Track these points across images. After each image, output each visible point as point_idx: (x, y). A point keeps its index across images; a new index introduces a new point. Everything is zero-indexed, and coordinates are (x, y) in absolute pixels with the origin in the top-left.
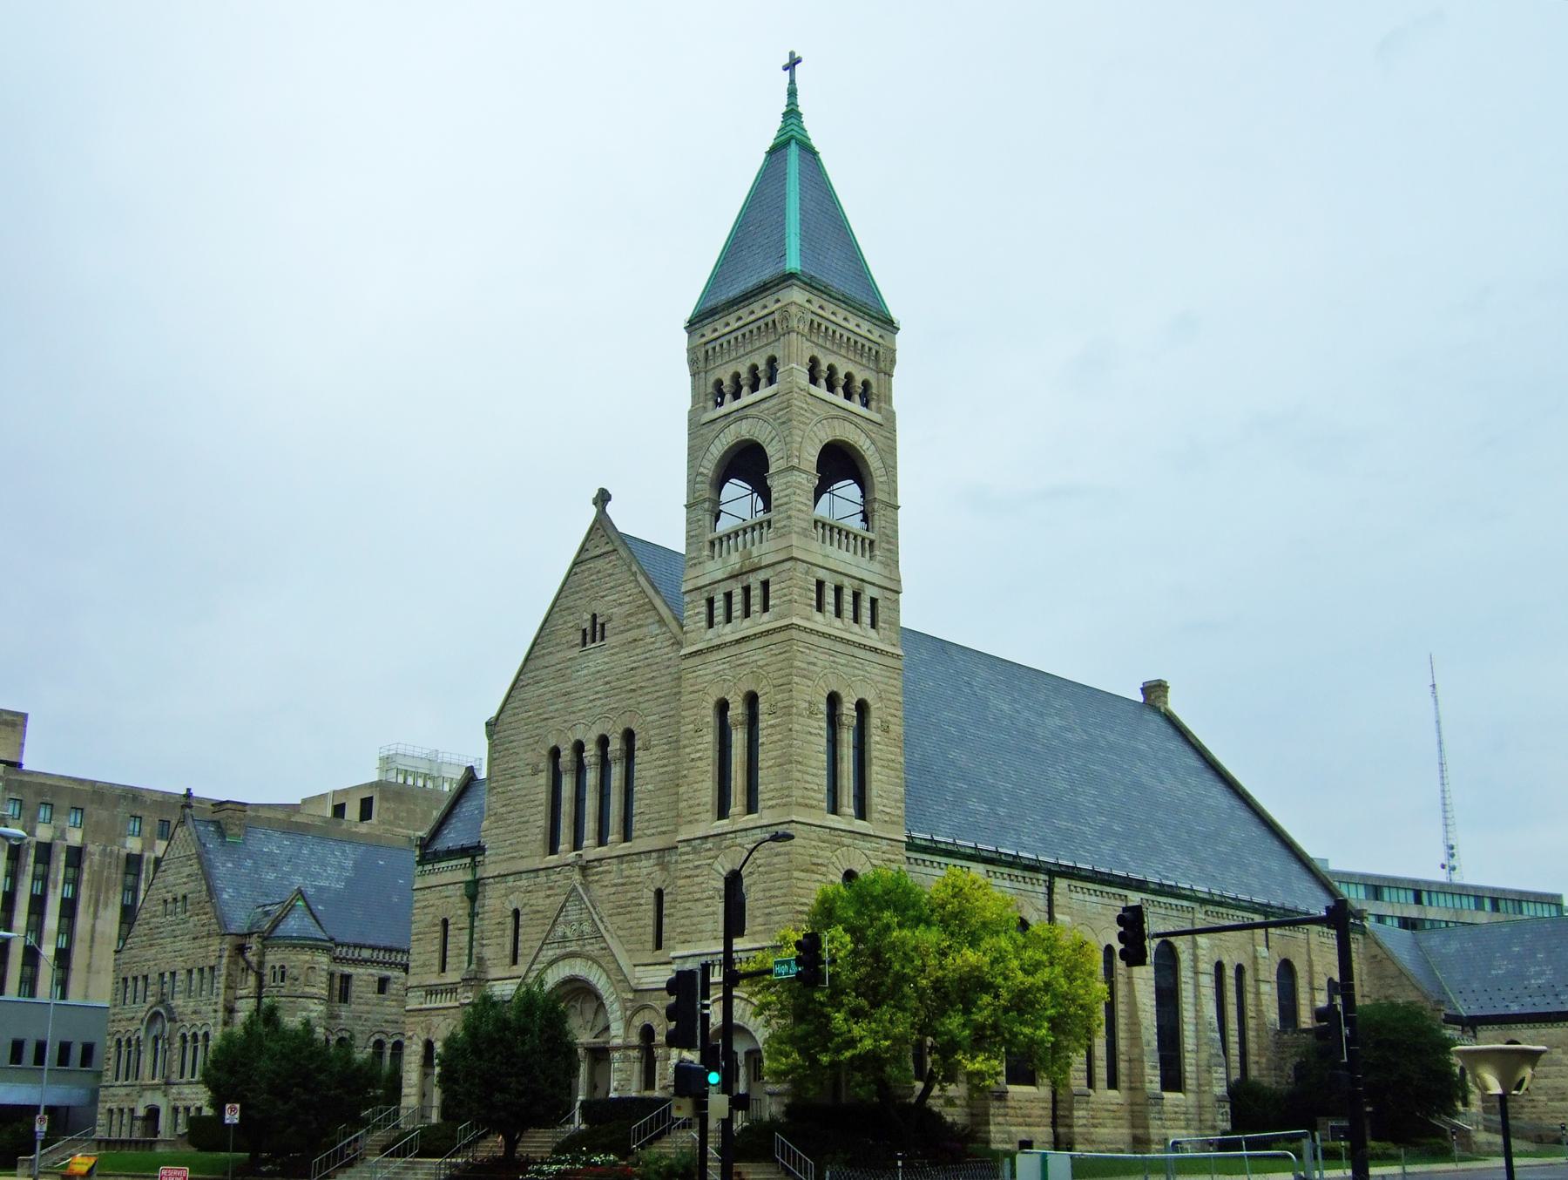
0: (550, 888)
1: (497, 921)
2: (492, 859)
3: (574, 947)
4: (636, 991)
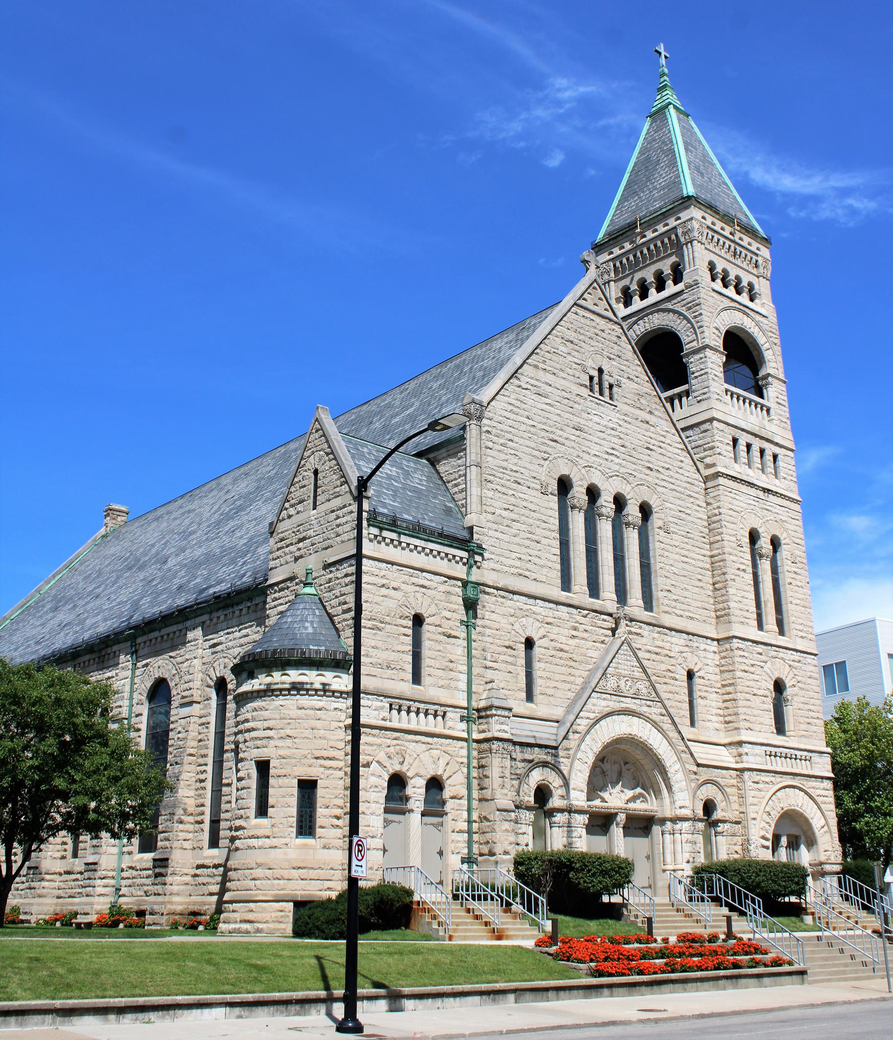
0: (575, 629)
1: (507, 644)
2: (492, 565)
3: (629, 704)
4: (698, 765)
